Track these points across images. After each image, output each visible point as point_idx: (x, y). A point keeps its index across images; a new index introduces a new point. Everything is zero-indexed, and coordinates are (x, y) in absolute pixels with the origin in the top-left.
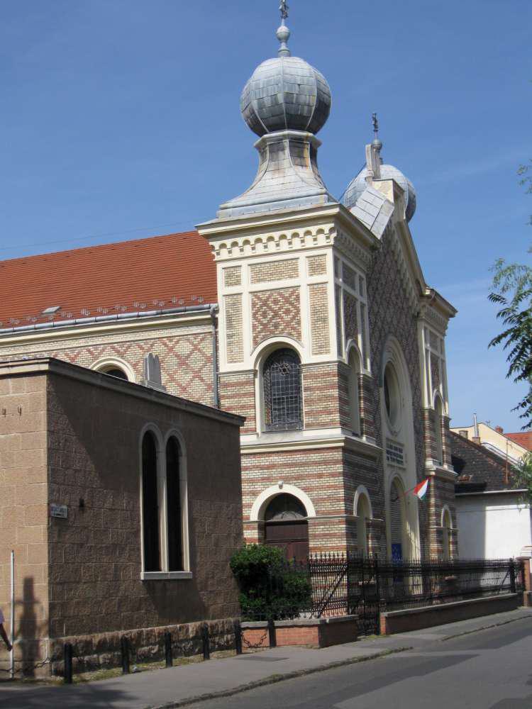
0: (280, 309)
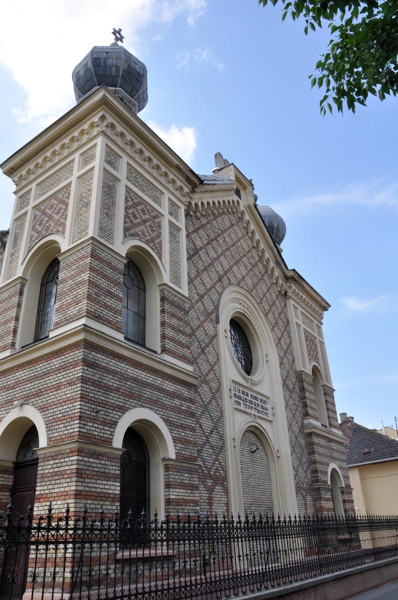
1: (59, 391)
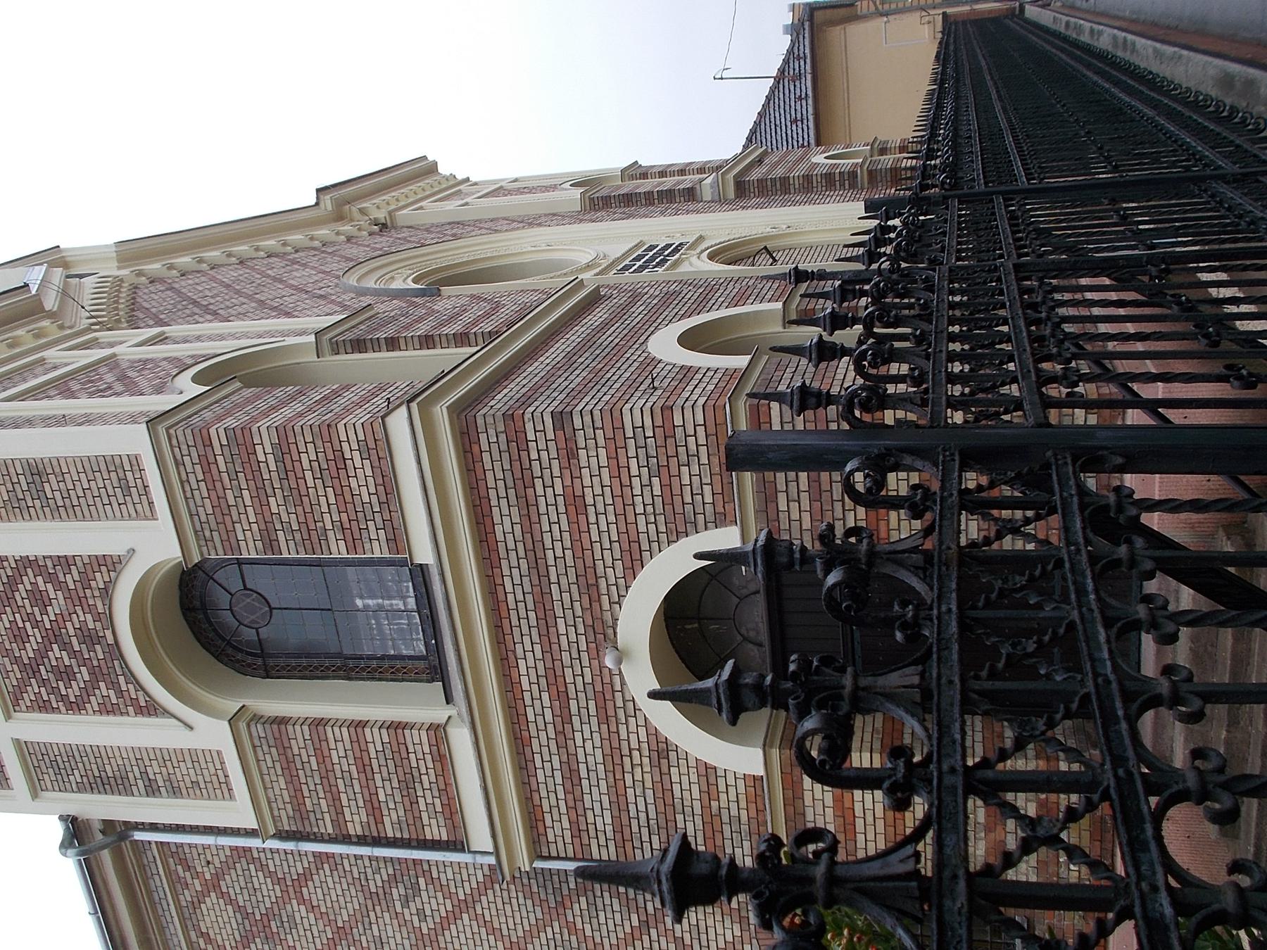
0: (36, 624)
1: (589, 500)
